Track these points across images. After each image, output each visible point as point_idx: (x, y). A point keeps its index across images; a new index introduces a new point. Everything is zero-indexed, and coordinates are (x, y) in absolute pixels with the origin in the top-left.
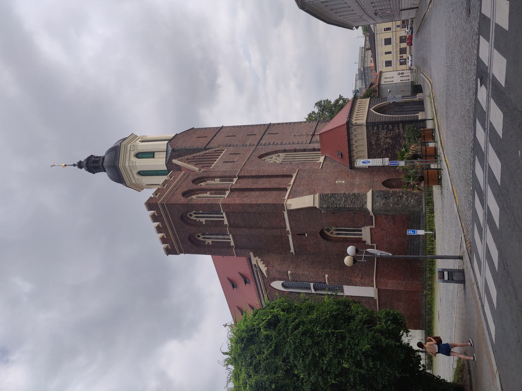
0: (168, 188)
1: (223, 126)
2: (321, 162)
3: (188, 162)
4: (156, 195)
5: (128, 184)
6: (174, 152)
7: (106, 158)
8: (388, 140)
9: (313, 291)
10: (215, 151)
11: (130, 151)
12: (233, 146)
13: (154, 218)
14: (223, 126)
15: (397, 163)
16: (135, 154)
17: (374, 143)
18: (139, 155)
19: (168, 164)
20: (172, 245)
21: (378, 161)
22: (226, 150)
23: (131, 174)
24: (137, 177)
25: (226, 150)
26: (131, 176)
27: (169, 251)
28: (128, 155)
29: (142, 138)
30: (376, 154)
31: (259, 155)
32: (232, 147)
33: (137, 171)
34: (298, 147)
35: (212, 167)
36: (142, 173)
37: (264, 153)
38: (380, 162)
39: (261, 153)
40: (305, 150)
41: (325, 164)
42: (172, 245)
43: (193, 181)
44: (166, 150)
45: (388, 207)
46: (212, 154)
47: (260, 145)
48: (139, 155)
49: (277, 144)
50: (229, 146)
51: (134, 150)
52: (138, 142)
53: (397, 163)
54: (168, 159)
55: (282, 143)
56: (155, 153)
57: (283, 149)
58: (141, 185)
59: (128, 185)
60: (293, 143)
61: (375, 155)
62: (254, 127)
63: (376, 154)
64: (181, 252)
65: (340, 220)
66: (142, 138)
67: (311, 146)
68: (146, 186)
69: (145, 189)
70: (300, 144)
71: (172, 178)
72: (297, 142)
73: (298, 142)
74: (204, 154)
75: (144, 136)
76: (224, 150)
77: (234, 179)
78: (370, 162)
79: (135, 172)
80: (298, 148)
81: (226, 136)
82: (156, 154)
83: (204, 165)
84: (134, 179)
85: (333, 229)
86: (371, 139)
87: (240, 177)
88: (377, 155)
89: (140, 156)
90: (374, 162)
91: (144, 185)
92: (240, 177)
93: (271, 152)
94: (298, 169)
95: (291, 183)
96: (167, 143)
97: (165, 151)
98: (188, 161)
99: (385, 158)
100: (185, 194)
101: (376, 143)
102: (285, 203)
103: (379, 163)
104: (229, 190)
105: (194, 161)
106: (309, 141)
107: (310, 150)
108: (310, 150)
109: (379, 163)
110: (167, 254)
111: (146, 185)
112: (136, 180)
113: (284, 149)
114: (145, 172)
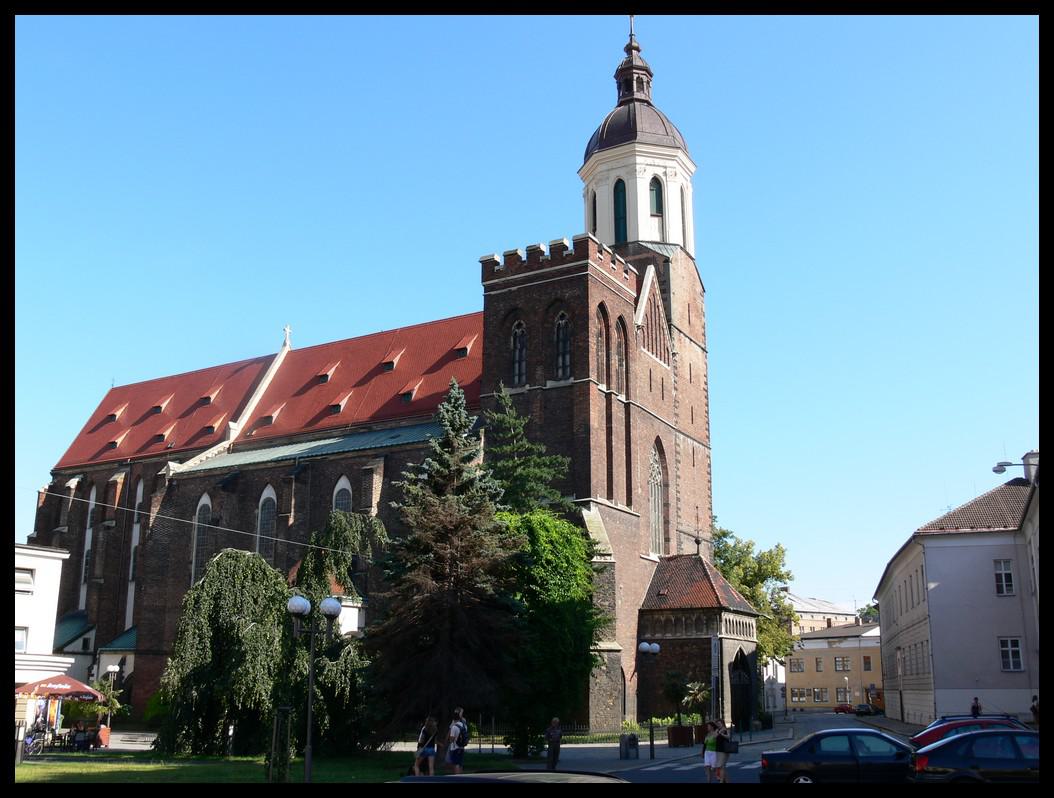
13: (558, 248)
17: (686, 649)
20: (499, 274)
22: (669, 368)
26: (614, 164)
27: (488, 266)
34: (672, 511)
36: (620, 190)
39: (663, 441)
40: (666, 522)
42: (499, 274)
43: (621, 318)
54: (649, 246)
55: (679, 477)
57: (670, 483)
60: (678, 499)
64: (487, 289)
67: (673, 534)
69: (583, 185)
73: (679, 509)
80: (671, 511)
92: (627, 406)
98: (652, 302)
100: (602, 306)
106: (681, 528)
107: (667, 532)
108: (667, 532)
114: (621, 194)
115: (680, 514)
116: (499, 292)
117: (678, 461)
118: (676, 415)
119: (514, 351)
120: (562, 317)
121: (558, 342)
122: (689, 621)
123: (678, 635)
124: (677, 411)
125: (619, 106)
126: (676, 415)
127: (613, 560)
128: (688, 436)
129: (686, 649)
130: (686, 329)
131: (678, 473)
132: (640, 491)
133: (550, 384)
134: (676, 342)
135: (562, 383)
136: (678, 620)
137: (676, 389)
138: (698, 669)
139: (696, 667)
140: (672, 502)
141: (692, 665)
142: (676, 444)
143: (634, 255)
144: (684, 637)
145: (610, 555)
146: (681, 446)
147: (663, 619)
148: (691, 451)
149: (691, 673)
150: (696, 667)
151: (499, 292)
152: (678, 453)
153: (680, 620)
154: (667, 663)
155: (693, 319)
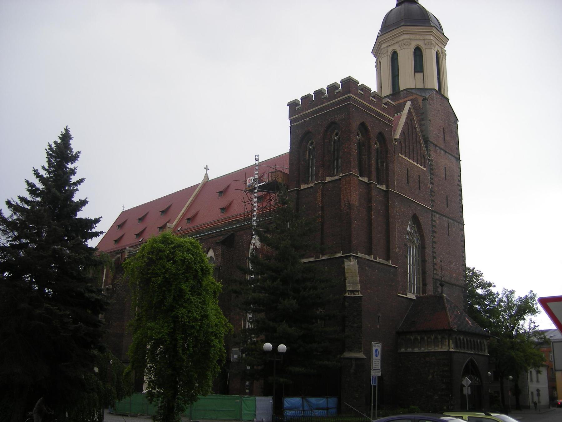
0: (371, 102)
1: (461, 161)
2: (406, 295)
3: (407, 123)
4: (362, 90)
5: (381, 39)
6: (423, 100)
7: (414, 6)
8: (431, 376)
10: (424, 156)
11: (424, 39)
12: (431, 178)
14: (461, 161)
15: (374, 383)
16: (420, 47)
18: (418, 53)
19: (408, 92)
21: (377, 364)
23: (394, 42)
24: (390, 50)
25: (425, 169)
26: (390, 43)
27: (293, 105)
28: (418, 37)
29: (442, 53)
31: (417, 215)
32: (429, 177)
33: (398, 50)
35: (400, 155)
36: (394, 57)
37: (421, 221)
38: (375, 367)
44: (425, 88)
46: (419, 152)
47: (432, 215)
48: (418, 53)
49: (434, 237)
50: (431, 173)
51: (425, 44)
52: (437, 48)
53: (374, 383)
57: (427, 246)
58: (380, 55)
59: (379, 38)
62: (459, 203)
64: (292, 121)
66: (442, 53)
68: (379, 62)
70: (434, 266)
71: (384, 105)
72: (435, 262)
74: (419, 142)
75: (446, 55)
76: (425, 168)
77: (384, 186)
78: (376, 356)
79: (397, 48)
81: (445, 168)
82: (419, 75)
83: (403, 145)
84: (387, 47)
85: (322, 311)
87: (387, 192)
90: (377, 361)
91: (380, 59)
93: (422, 229)
94: (397, 266)
95: (378, 259)
96: (434, 89)
99: (380, 372)
102: (352, 254)
103: (375, 366)
104: (369, 181)
105: (408, 130)
106: (436, 277)
109: (375, 366)
110: (290, 104)
111: (380, 61)
112: (386, 48)
113: (426, 246)
115: (436, 267)
116: (298, 123)
117: (434, 232)
118: (433, 201)
119: (309, 160)
120: (337, 135)
121: (334, 152)
122: (429, 340)
123: (423, 350)
124: (433, 198)
125: (397, 5)
126: (433, 201)
127: (360, 295)
128: (443, 216)
130: (441, 144)
131: (434, 240)
132: (397, 250)
133: (328, 179)
134: (432, 153)
135: (336, 178)
136: (422, 339)
137: (432, 183)
140: (429, 259)
142: (432, 220)
143: (403, 98)
144: (426, 351)
145: (358, 291)
146: (437, 222)
147: (412, 338)
148: (446, 225)
149: (431, 376)
151: (298, 123)
152: (435, 226)
155: (447, 139)
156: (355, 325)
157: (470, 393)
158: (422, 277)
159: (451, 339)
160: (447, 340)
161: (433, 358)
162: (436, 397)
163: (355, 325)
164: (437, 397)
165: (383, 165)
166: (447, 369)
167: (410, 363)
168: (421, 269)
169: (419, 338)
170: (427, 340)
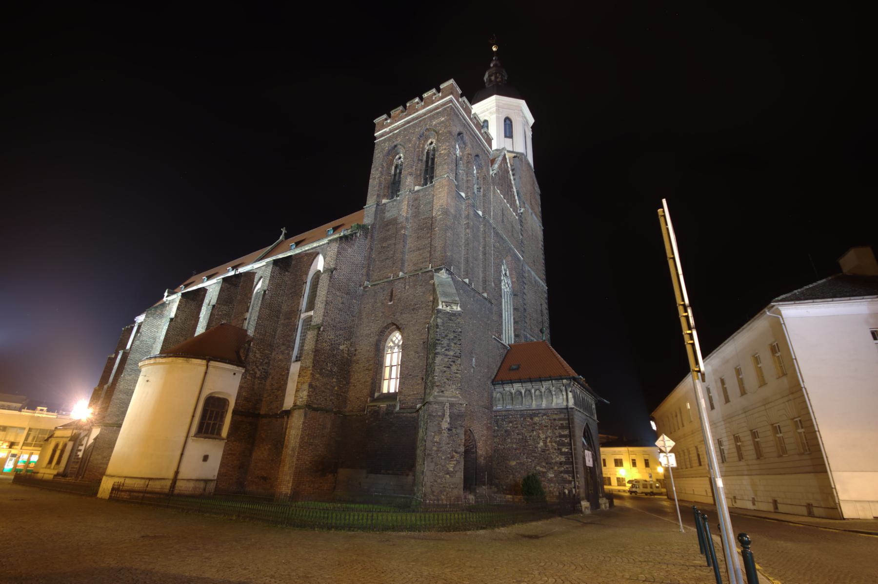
8: (541, 444)
9: (303, 316)
30: (516, 424)
41: (500, 344)
45: (433, 434)
56: (511, 139)
61: (515, 423)
63: (516, 424)
65: (412, 354)
82: (510, 140)
86: (542, 416)
88: (515, 426)
89: (508, 122)
97: (513, 149)
101: (535, 424)
129: (536, 419)
138: (549, 440)
139: (546, 438)
141: (542, 436)
150: (546, 438)
153: (530, 391)
154: (518, 434)
156: (452, 353)
157: (675, 465)
158: (514, 327)
159: (570, 392)
160: (564, 393)
161: (544, 417)
162: (551, 475)
163: (452, 353)
164: (553, 475)
165: (480, 191)
166: (566, 432)
167: (511, 425)
168: (512, 318)
169: (523, 392)
170: (535, 392)
